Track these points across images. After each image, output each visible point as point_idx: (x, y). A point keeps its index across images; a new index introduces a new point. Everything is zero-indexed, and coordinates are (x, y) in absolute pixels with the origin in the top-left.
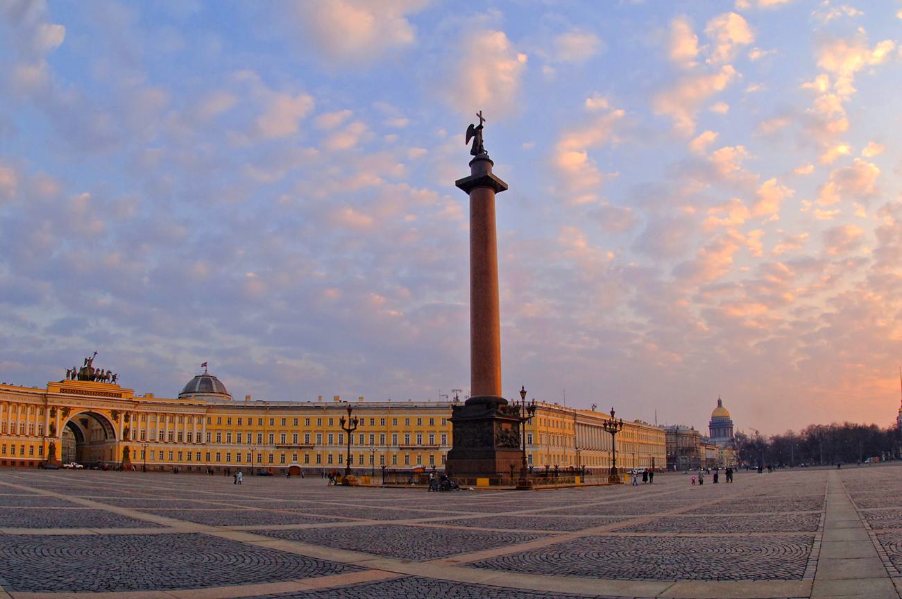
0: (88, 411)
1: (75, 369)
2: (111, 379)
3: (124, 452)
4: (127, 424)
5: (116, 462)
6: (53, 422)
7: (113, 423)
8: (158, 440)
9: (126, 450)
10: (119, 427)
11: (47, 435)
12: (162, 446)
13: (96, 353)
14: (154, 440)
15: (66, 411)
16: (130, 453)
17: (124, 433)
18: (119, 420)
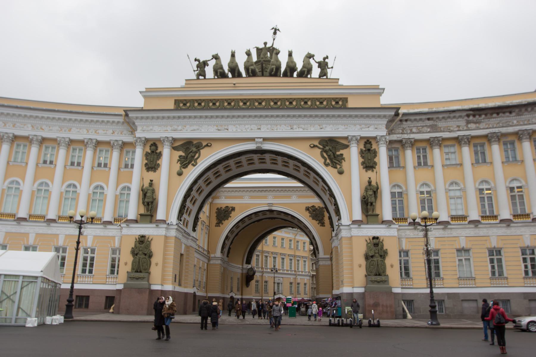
0: (251, 146)
1: (216, 57)
2: (316, 72)
3: (367, 257)
4: (370, 174)
5: (346, 289)
6: (151, 184)
7: (328, 174)
8: (474, 215)
9: (376, 251)
10: (347, 187)
11: (132, 215)
12: (494, 235)
13: (275, 31)
14: (463, 218)
15: (189, 150)
16: (388, 261)
18: (344, 164)
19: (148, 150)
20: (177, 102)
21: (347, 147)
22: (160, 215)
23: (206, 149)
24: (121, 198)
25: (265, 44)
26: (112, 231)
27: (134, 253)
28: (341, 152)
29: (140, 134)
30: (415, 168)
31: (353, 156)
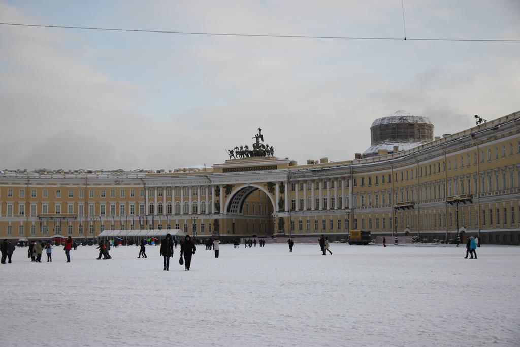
3: (279, 224)
6: (218, 201)
13: (260, 129)
15: (228, 188)
17: (279, 204)
19: (216, 188)
20: (224, 169)
21: (275, 185)
22: (221, 212)
23: (234, 187)
24: (210, 206)
25: (258, 134)
26: (208, 217)
27: (214, 224)
28: (274, 187)
29: (212, 184)
30: (299, 190)
31: (277, 188)
